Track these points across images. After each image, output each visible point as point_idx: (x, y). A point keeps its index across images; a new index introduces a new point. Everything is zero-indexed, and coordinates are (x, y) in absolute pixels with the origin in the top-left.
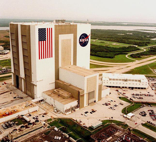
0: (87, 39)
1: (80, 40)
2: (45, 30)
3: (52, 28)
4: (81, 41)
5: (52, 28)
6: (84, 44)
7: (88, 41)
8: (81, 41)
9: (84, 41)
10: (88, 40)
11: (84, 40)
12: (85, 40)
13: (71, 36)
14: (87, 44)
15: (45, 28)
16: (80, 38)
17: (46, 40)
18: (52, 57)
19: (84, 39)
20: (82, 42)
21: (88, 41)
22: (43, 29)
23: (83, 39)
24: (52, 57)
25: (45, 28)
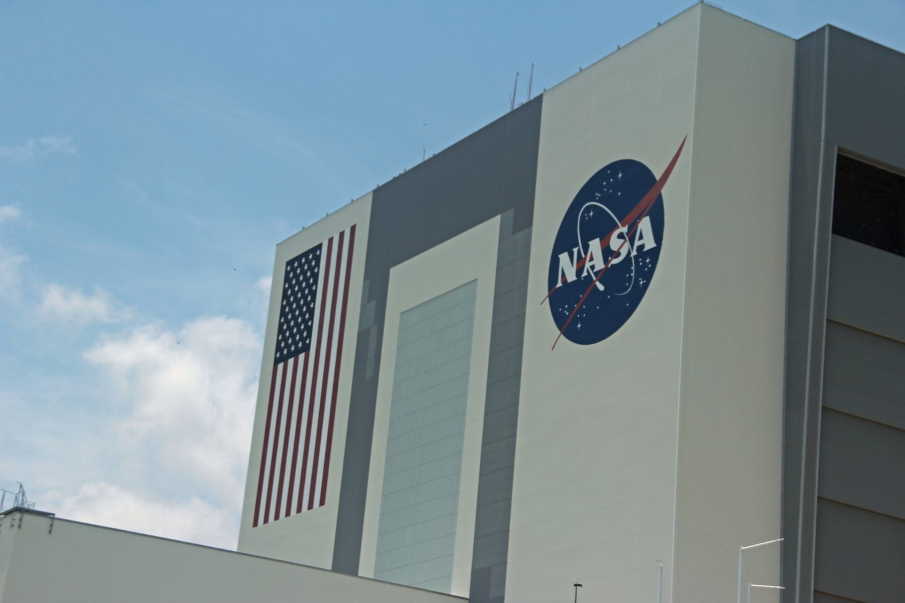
0: (645, 225)
1: (564, 257)
2: (318, 259)
3: (353, 229)
4: (571, 277)
5: (353, 229)
6: (594, 310)
7: (649, 243)
9: (599, 265)
11: (608, 253)
12: (614, 243)
15: (319, 247)
16: (565, 241)
17: (306, 349)
18: (322, 503)
20: (583, 283)
21: (654, 254)
22: (306, 254)
23: (595, 245)
24: (322, 503)
25: (319, 247)
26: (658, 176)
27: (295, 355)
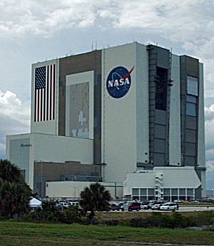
0: (127, 79)
1: (110, 82)
4: (112, 86)
6: (118, 93)
7: (128, 83)
8: (112, 86)
9: (118, 84)
10: (130, 82)
12: (121, 81)
13: (88, 77)
14: (126, 92)
16: (109, 79)
17: (45, 88)
19: (119, 79)
20: (114, 87)
21: (129, 85)
23: (116, 81)
26: (129, 71)
27: (42, 89)
